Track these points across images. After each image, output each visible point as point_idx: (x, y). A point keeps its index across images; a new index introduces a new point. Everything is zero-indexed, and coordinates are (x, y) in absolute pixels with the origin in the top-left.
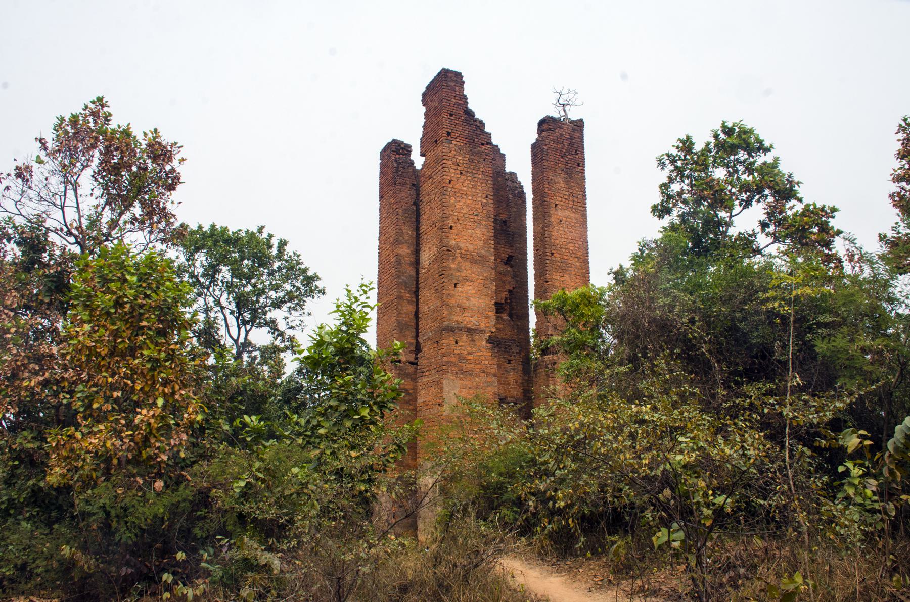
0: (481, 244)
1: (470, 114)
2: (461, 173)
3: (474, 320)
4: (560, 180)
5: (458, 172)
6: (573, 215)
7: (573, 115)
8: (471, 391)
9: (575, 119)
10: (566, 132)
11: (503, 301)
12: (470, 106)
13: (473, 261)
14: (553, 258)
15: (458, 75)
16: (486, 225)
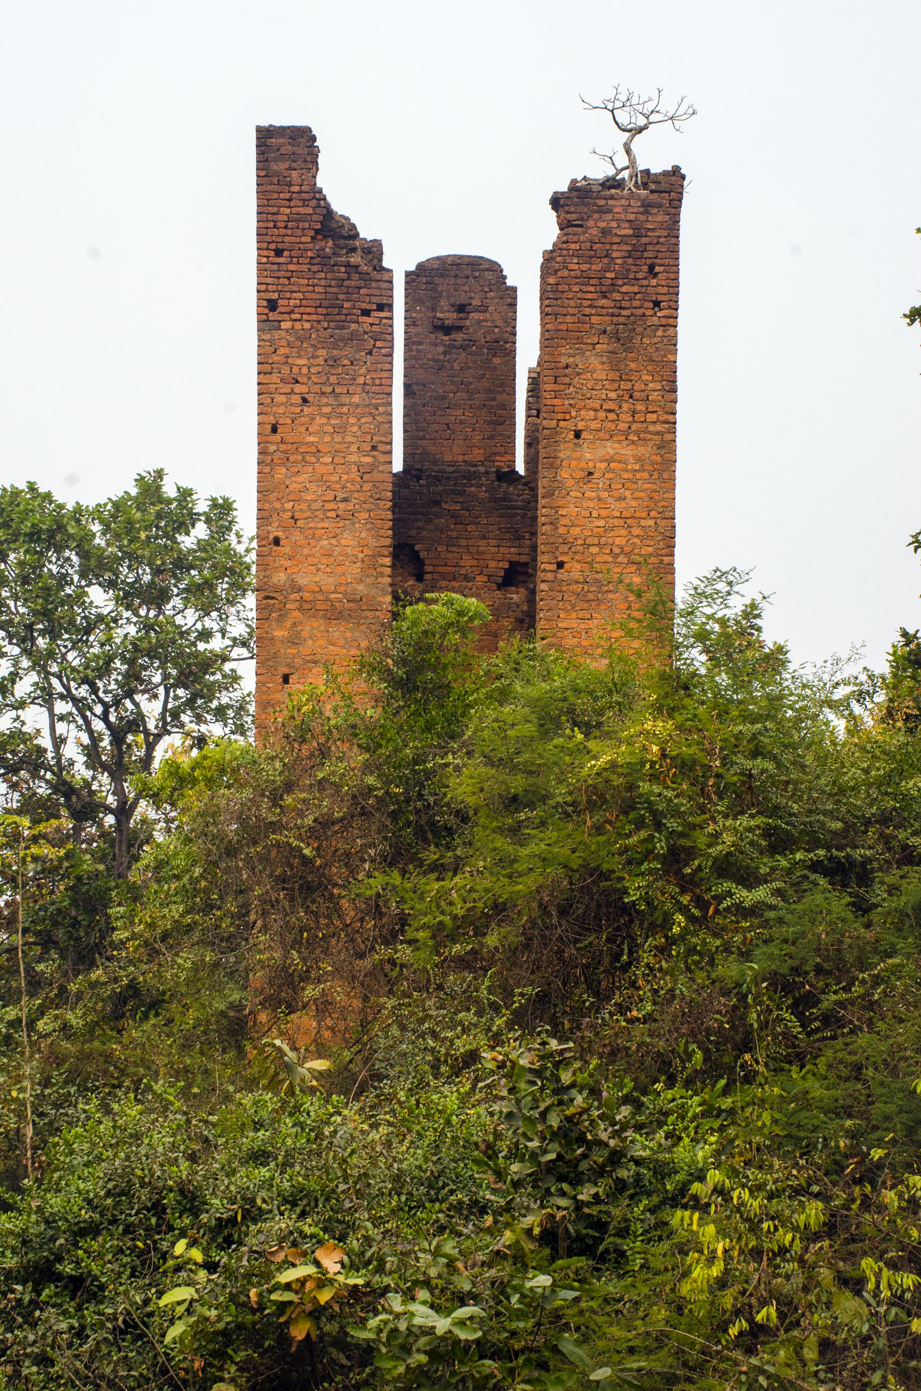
0: (356, 569)
2: (305, 400)
4: (594, 362)
5: (296, 399)
6: (628, 452)
7: (654, 156)
9: (656, 169)
10: (618, 220)
12: (339, 206)
13: (334, 615)
14: (562, 574)
16: (369, 520)
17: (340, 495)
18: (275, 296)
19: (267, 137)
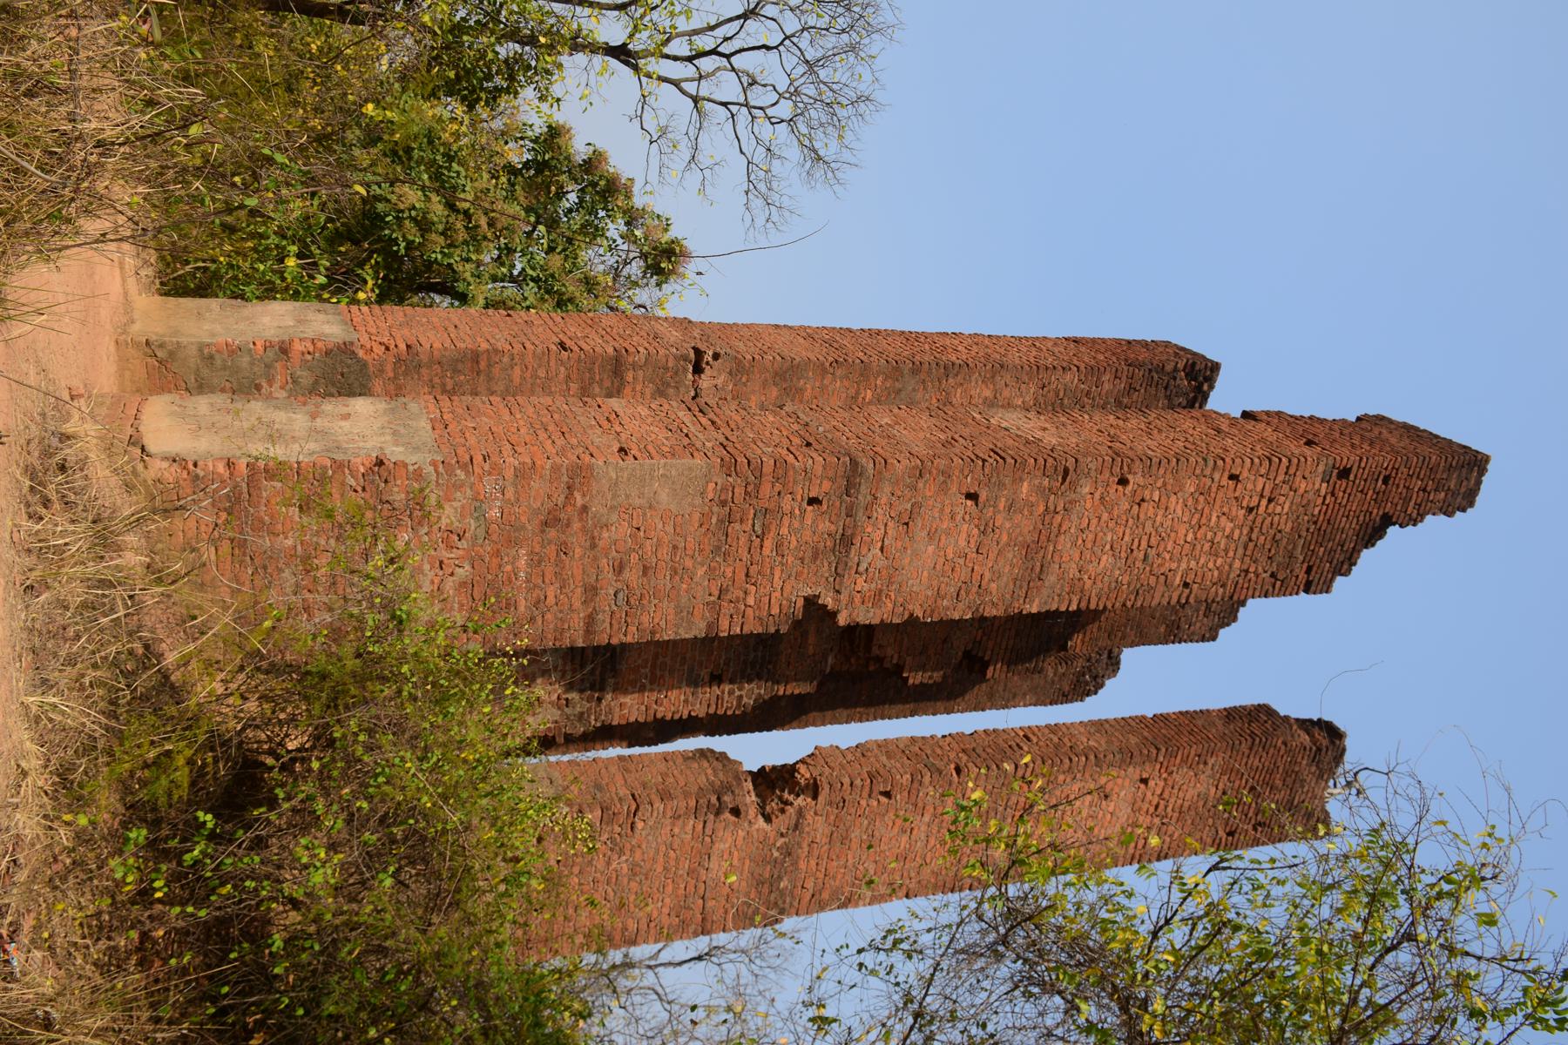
1: (1372, 534)
3: (872, 557)
8: (664, 553)
11: (875, 651)
15: (1466, 499)
17: (1152, 552)
18: (1352, 477)
19: (1472, 464)
